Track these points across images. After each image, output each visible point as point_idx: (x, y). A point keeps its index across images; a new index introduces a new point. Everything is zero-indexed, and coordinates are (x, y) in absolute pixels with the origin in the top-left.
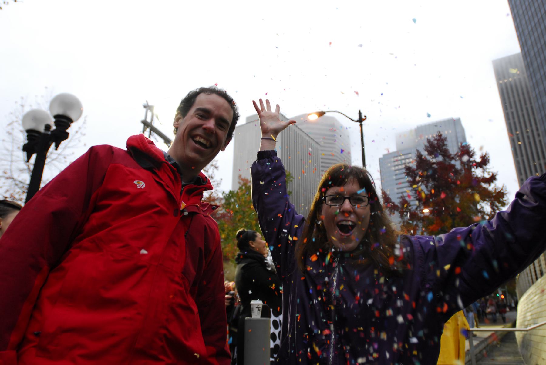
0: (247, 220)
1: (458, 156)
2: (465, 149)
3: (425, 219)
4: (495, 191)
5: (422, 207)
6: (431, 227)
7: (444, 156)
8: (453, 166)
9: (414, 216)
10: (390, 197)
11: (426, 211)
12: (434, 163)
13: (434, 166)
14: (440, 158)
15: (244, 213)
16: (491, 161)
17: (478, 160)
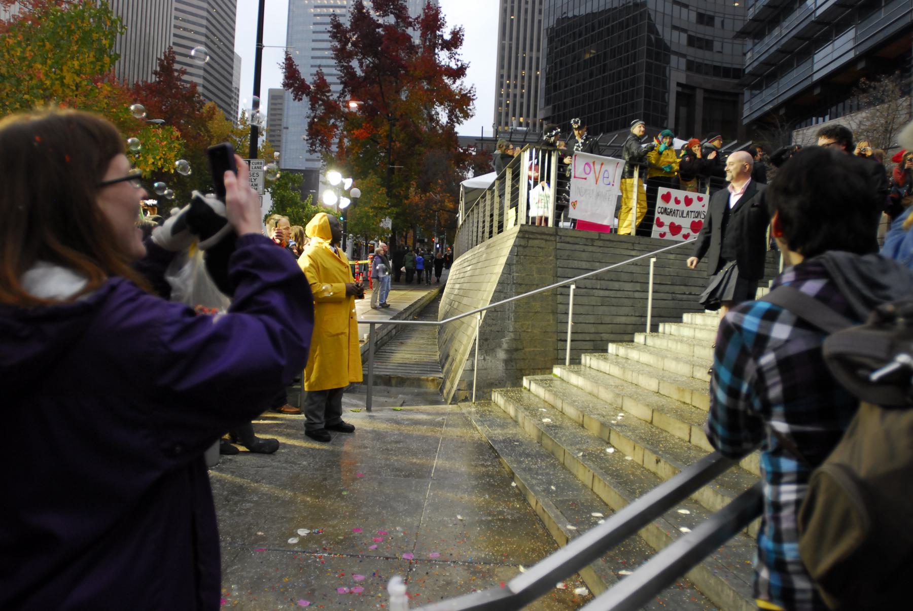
0: (26, 97)
1: (418, 23)
2: (432, 13)
3: (349, 117)
4: (460, 92)
5: (348, 97)
6: (356, 132)
7: (397, 17)
8: (409, 38)
9: (332, 109)
11: (353, 105)
12: (379, 26)
13: (380, 30)
14: (391, 20)
15: (19, 82)
16: (464, 42)
17: (447, 37)
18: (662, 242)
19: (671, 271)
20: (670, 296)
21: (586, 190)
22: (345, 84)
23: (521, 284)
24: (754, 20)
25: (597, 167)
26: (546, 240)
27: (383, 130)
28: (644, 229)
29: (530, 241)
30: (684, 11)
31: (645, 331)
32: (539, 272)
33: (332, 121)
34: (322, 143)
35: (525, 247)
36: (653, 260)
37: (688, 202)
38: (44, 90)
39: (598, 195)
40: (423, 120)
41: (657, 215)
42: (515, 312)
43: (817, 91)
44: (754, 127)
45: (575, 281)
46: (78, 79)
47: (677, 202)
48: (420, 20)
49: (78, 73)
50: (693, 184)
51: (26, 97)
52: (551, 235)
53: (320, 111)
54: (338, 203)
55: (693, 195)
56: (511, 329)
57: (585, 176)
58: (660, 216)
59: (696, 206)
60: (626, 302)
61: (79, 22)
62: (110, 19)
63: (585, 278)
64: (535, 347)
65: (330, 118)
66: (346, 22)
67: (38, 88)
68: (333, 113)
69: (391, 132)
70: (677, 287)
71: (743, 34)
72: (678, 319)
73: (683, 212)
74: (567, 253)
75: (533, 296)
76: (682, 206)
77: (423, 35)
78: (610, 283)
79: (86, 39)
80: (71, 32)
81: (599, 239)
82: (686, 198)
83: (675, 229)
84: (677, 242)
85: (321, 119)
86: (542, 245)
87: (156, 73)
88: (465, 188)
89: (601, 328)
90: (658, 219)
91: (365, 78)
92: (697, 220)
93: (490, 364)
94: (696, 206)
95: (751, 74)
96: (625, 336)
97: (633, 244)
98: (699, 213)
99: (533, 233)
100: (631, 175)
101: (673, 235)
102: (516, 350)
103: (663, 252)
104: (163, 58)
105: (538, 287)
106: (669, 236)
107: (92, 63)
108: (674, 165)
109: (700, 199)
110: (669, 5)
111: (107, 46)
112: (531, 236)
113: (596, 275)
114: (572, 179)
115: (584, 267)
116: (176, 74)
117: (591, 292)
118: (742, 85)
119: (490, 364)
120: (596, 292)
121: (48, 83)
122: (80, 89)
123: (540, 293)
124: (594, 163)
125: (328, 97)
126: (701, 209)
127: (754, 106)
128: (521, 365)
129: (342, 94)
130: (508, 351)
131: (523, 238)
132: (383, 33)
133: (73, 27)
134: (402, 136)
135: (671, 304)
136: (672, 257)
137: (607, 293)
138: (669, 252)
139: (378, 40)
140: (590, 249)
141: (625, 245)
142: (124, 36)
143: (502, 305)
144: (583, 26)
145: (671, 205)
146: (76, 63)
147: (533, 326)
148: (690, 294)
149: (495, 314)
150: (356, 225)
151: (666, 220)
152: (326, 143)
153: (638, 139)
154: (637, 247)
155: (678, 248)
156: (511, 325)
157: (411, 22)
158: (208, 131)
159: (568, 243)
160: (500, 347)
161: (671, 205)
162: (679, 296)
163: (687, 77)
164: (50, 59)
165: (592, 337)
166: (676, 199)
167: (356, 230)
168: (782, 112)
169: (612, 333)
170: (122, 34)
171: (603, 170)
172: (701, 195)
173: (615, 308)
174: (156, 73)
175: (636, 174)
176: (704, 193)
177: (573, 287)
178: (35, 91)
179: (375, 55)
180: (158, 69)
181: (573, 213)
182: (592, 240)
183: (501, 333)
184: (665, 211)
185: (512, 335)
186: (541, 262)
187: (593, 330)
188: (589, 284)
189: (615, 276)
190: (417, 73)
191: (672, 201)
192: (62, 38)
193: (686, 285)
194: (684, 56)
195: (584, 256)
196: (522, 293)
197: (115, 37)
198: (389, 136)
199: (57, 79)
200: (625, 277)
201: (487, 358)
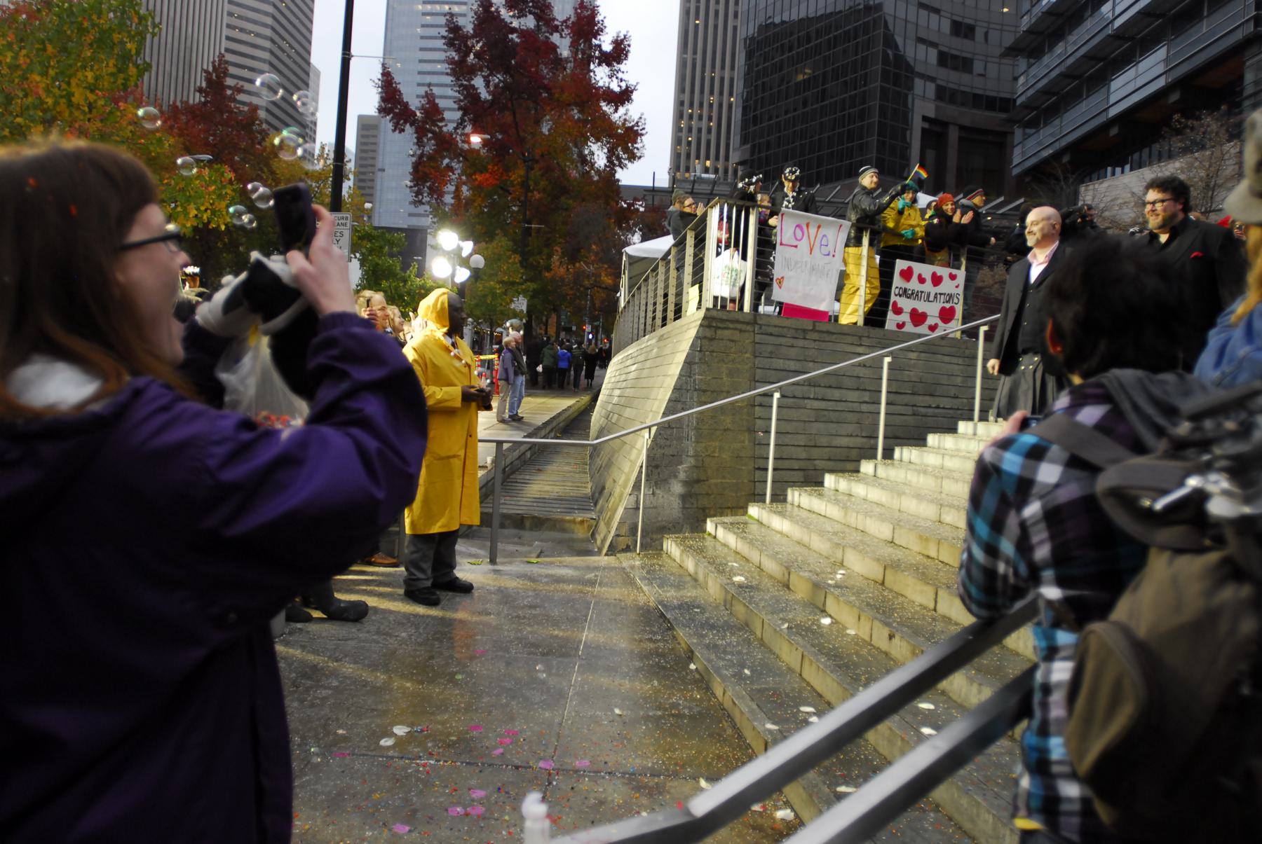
0: (19, 120)
1: (567, 27)
3: (469, 157)
4: (624, 124)
5: (469, 129)
6: (479, 177)
7: (538, 18)
8: (554, 48)
9: (446, 144)
10: (400, 87)
11: (476, 139)
12: (513, 30)
13: (514, 36)
14: (530, 22)
15: (9, 99)
16: (630, 56)
17: (607, 47)
18: (900, 335)
19: (912, 375)
20: (909, 410)
21: (796, 263)
22: (465, 111)
23: (704, 391)
24: (1030, 31)
25: (813, 231)
26: (741, 331)
27: (517, 175)
28: (875, 316)
29: (719, 332)
30: (934, 17)
31: (874, 457)
32: (731, 374)
33: (446, 161)
34: (432, 191)
35: (711, 339)
36: (887, 360)
37: (937, 280)
38: (44, 111)
39: (813, 269)
40: (572, 162)
41: (893, 298)
42: (697, 429)
43: (1114, 131)
44: (1027, 180)
45: (780, 388)
46: (92, 97)
47: (922, 280)
48: (569, 23)
49: (92, 89)
50: (942, 255)
51: (19, 120)
52: (748, 323)
53: (429, 148)
54: (453, 275)
55: (944, 272)
56: (691, 453)
57: (795, 243)
58: (898, 299)
59: (947, 286)
60: (850, 417)
61: (94, 17)
62: (137, 13)
63: (794, 384)
64: (724, 477)
65: (443, 158)
66: (467, 24)
67: (35, 107)
68: (447, 150)
69: (527, 177)
70: (921, 398)
71: (1014, 51)
72: (920, 441)
73: (929, 295)
74: (770, 348)
75: (721, 407)
76: (928, 286)
77: (574, 45)
78: (828, 390)
79: (103, 41)
80: (82, 31)
81: (814, 330)
82: (934, 275)
83: (918, 318)
84: (920, 336)
85: (431, 158)
86: (735, 338)
87: (200, 90)
88: (629, 256)
89: (815, 453)
90: (895, 304)
91: (493, 102)
92: (948, 306)
93: (661, 500)
94: (947, 286)
95: (1027, 106)
96: (848, 464)
97: (860, 337)
98: (950, 297)
99: (722, 320)
100: (858, 243)
101: (916, 326)
102: (698, 481)
103: (901, 349)
104: (211, 69)
105: (729, 394)
106: (909, 328)
107: (112, 74)
108: (917, 229)
109: (953, 277)
110: (913, 9)
111: (134, 51)
112: (720, 325)
113: (809, 379)
114: (778, 246)
115: (793, 368)
116: (229, 92)
117: (801, 402)
118: (1013, 122)
119: (661, 500)
120: (809, 403)
121: (50, 101)
122: (94, 111)
123: (732, 403)
124: (808, 225)
125: (440, 128)
126: (953, 291)
127: (1028, 150)
128: (704, 502)
129: (461, 123)
130: (686, 483)
131: (709, 326)
132: (518, 40)
133: (86, 24)
134: (543, 183)
135: (910, 420)
136: (913, 355)
137: (823, 405)
138: (908, 349)
139: (511, 50)
140: (801, 343)
141: (849, 339)
142: (156, 39)
143: (679, 419)
144: (795, 36)
145: (914, 285)
146: (90, 75)
147: (721, 448)
148: (938, 407)
149: (669, 432)
150: (477, 305)
151: (906, 304)
152: (437, 192)
153: (868, 192)
154: (865, 341)
155: (922, 343)
156: (690, 447)
157: (557, 27)
158: (273, 173)
159: (771, 335)
160: (676, 477)
161: (914, 285)
162: (923, 410)
163: (937, 108)
164: (53, 67)
165: (802, 464)
166: (920, 276)
167: (478, 313)
168: (1066, 159)
169: (829, 460)
170: (154, 35)
171: (820, 235)
172: (954, 272)
173: (834, 425)
174: (200, 90)
175: (866, 241)
176: (959, 268)
177: (777, 395)
178: (31, 113)
179: (507, 70)
180: (204, 85)
181: (779, 294)
182: (804, 330)
183: (677, 458)
184: (905, 293)
185: (692, 460)
186: (733, 361)
187: (804, 455)
188: (798, 391)
189: (835, 381)
190: (565, 96)
191: (915, 278)
192: (70, 39)
193: (931, 395)
194: (932, 79)
195: (793, 352)
196: (706, 403)
197: (145, 39)
198: (525, 185)
199: (62, 97)
200: (848, 382)
201: (658, 492)
